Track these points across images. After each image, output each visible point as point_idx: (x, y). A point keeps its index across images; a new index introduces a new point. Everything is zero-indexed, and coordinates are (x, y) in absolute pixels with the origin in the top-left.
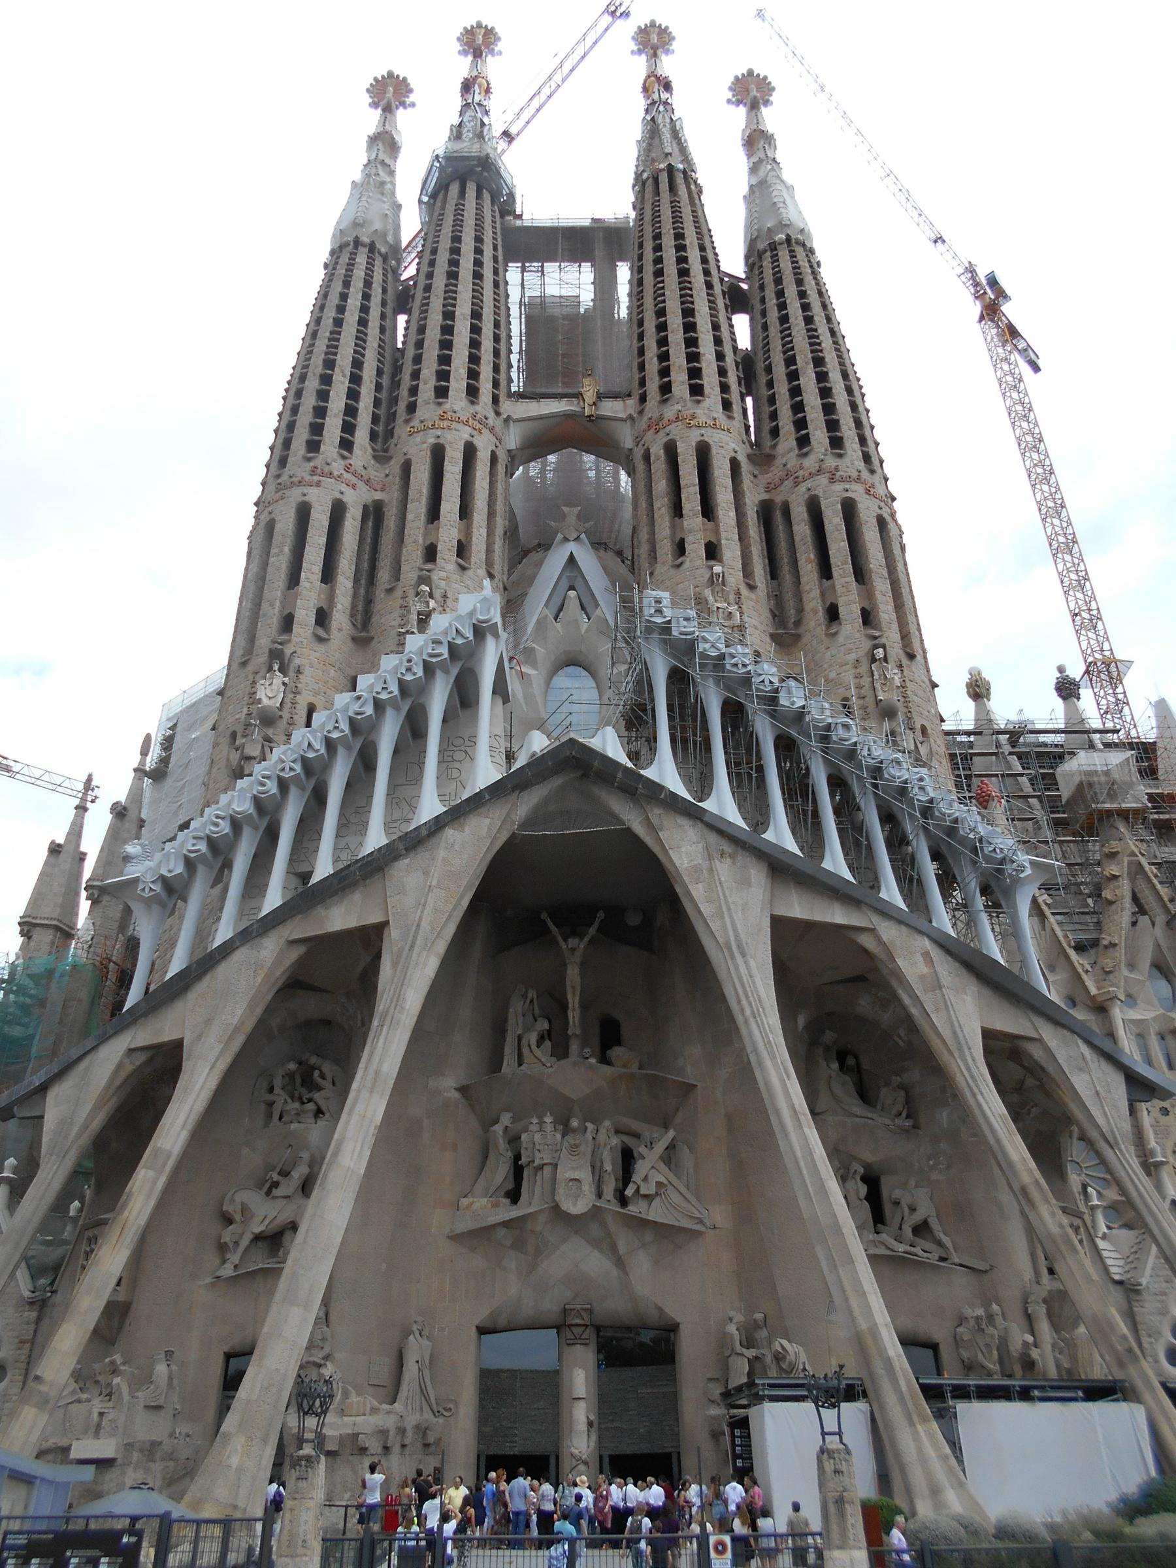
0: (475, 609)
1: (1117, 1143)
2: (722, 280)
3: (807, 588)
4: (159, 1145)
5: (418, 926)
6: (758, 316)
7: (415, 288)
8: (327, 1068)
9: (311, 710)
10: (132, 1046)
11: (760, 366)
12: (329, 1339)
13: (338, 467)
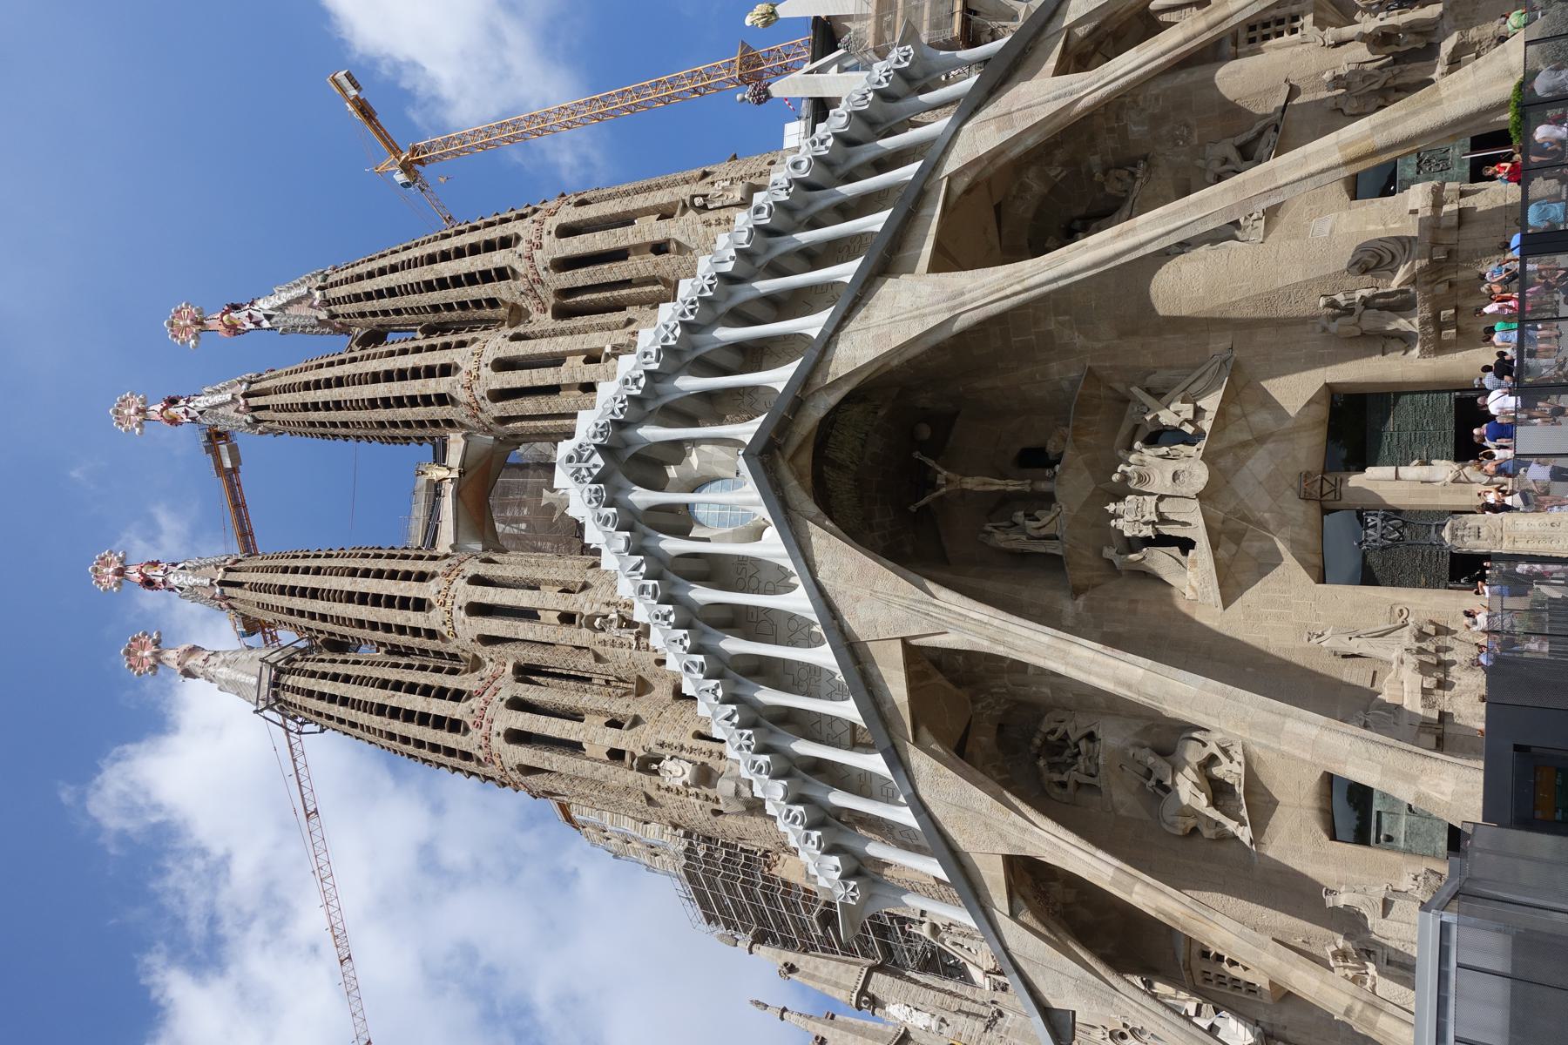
3: (634, 272)
4: (1109, 879)
8: (1045, 728)
9: (699, 736)
10: (1007, 913)
11: (432, 318)
13: (476, 703)
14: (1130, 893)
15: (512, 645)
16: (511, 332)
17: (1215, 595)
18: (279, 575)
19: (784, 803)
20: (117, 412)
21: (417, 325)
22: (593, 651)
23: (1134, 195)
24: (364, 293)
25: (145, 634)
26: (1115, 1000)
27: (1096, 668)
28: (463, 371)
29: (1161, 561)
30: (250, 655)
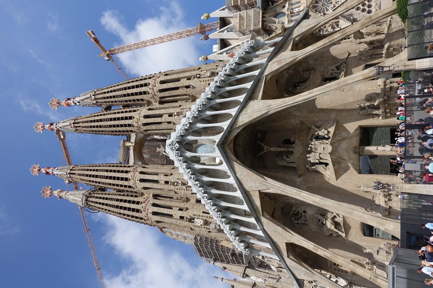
3: (181, 93)
7: (99, 186)
10: (287, 256)
11: (125, 103)
13: (143, 205)
14: (317, 252)
15: (152, 189)
16: (148, 108)
17: (334, 177)
18: (86, 171)
19: (229, 230)
20: (36, 127)
21: (120, 105)
22: (174, 191)
24: (106, 97)
25: (47, 187)
26: (314, 276)
27: (308, 199)
28: (135, 118)
29: (320, 168)
30: (78, 193)
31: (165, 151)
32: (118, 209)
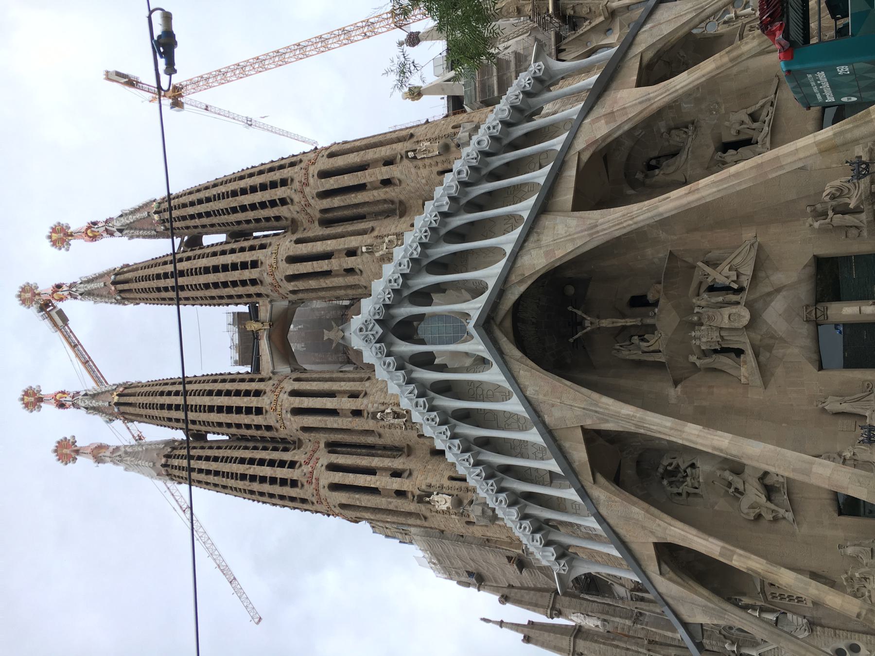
0: (397, 384)
1: (702, 7)
2: (184, 252)
3: (372, 197)
4: (718, 554)
5: (584, 409)
6: (205, 230)
9: (452, 478)
10: (659, 572)
11: (236, 228)
12: (828, 454)
13: (306, 469)
14: (731, 561)
16: (294, 237)
23: (688, 146)
24: (189, 215)
31: (344, 336)
32: (245, 482)
